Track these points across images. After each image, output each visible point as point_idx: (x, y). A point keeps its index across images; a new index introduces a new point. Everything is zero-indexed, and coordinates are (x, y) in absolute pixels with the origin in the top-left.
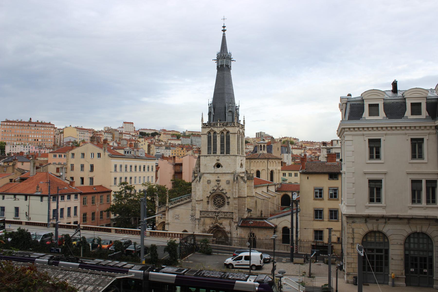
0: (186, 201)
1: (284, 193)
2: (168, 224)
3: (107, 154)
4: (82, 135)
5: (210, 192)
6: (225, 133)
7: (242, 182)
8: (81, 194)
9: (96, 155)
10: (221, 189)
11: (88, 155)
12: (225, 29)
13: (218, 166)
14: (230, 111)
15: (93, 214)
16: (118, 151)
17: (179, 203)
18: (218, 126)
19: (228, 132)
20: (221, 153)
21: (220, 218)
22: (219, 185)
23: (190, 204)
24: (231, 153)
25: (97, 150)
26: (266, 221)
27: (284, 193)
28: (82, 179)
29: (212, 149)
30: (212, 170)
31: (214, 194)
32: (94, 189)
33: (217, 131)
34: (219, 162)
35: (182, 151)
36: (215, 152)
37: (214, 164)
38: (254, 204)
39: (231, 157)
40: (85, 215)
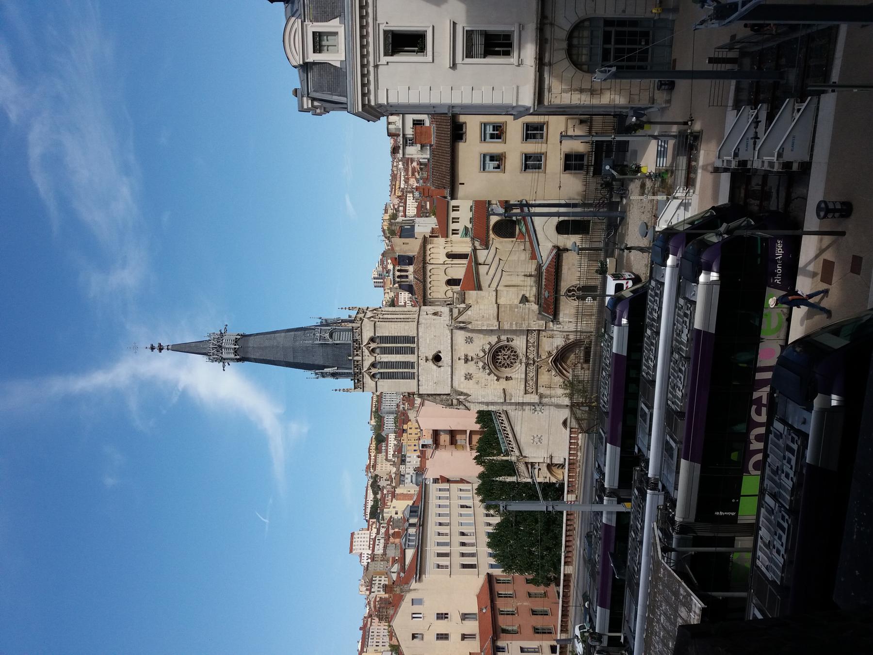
0: (506, 422)
1: (491, 232)
2: (551, 457)
3: (414, 585)
4: (375, 640)
5: (489, 374)
6: (373, 345)
7: (469, 312)
8: (494, 641)
9: (416, 608)
10: (482, 354)
11: (417, 626)
12: (156, 346)
13: (437, 358)
14: (331, 336)
15: (534, 613)
16: (408, 560)
17: (510, 436)
18: (359, 358)
19: (372, 340)
20: (413, 352)
21: (538, 356)
22: (475, 357)
23: (512, 414)
24: (411, 334)
25: (406, 607)
27: (491, 232)
28: (464, 637)
29: (407, 371)
30: (446, 370)
31: (492, 367)
32: (484, 611)
33: (370, 362)
34: (430, 357)
35: (409, 431)
36: (411, 365)
37: (435, 367)
38: (512, 289)
39: (420, 334)
40: (536, 631)
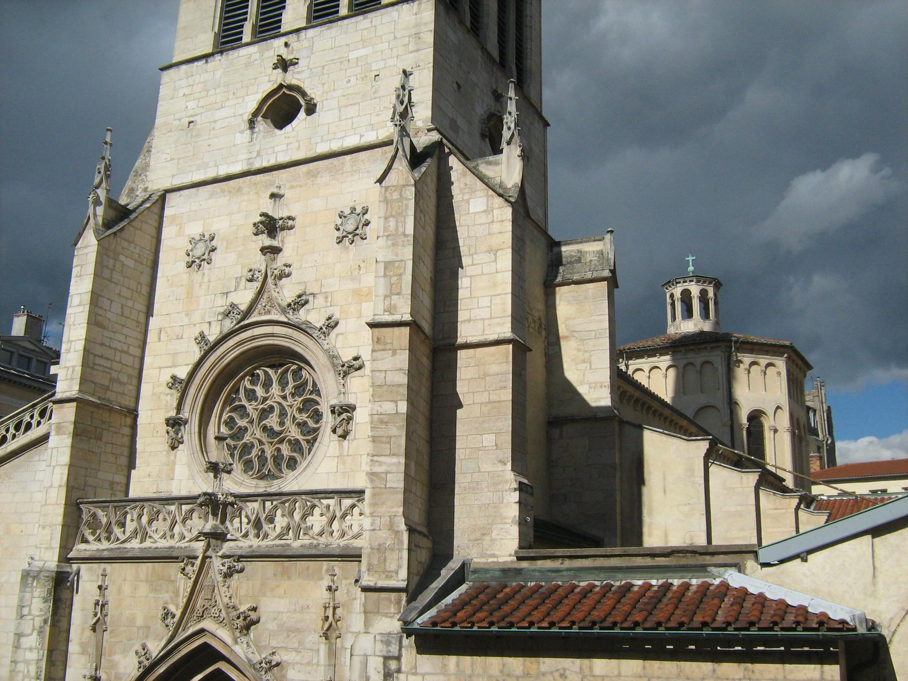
10: (288, 292)
26: (734, 579)
31: (229, 351)
34: (292, 77)
37: (253, 106)
